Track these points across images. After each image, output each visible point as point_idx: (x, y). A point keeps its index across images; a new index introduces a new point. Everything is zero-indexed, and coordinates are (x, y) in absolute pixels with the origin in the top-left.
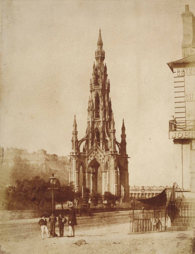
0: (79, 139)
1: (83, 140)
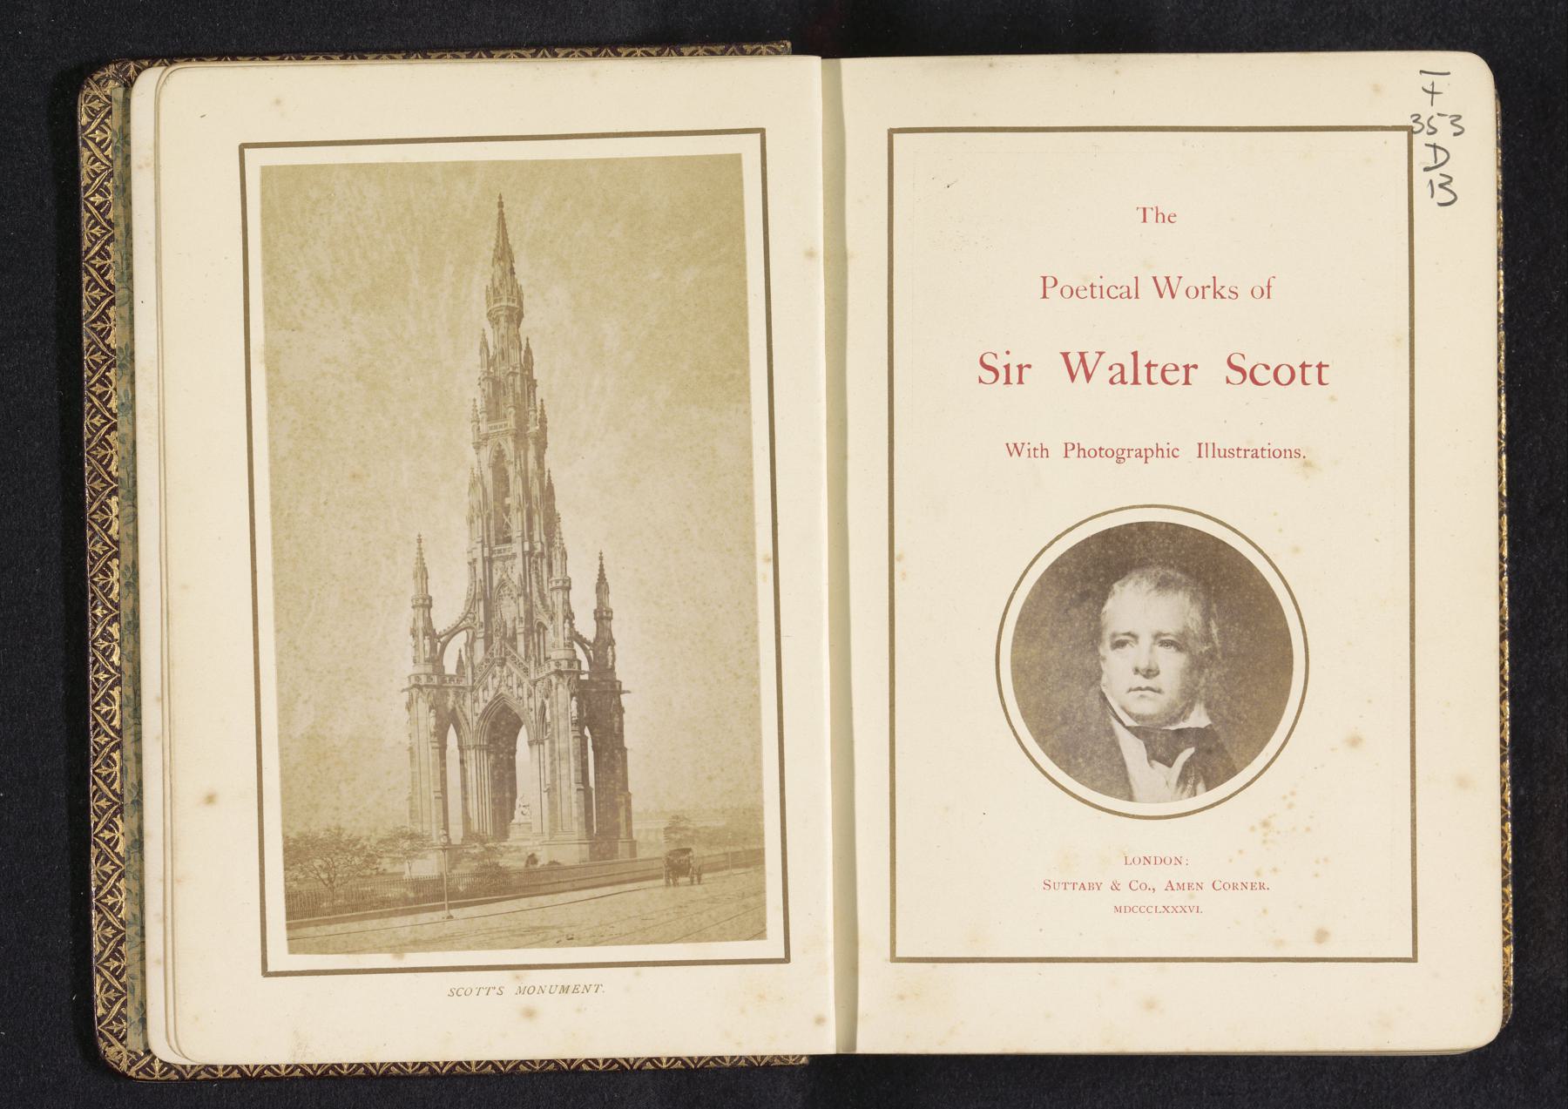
0: (440, 626)
1: (452, 633)
